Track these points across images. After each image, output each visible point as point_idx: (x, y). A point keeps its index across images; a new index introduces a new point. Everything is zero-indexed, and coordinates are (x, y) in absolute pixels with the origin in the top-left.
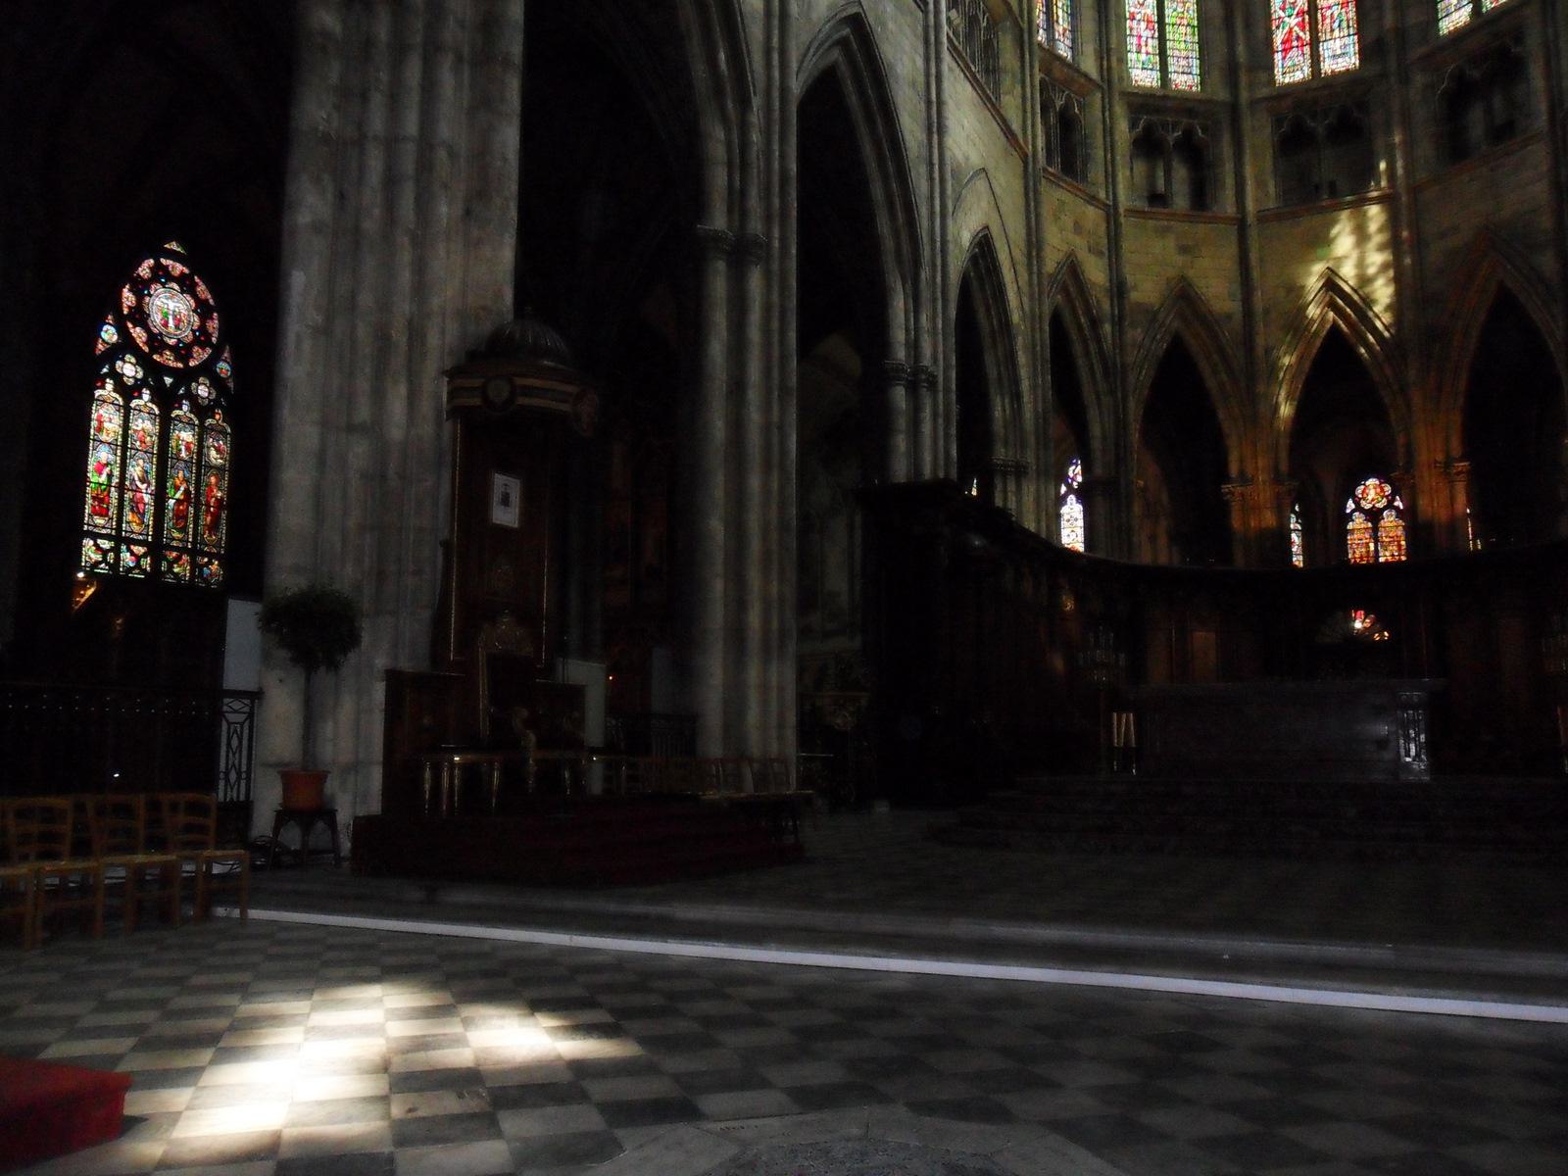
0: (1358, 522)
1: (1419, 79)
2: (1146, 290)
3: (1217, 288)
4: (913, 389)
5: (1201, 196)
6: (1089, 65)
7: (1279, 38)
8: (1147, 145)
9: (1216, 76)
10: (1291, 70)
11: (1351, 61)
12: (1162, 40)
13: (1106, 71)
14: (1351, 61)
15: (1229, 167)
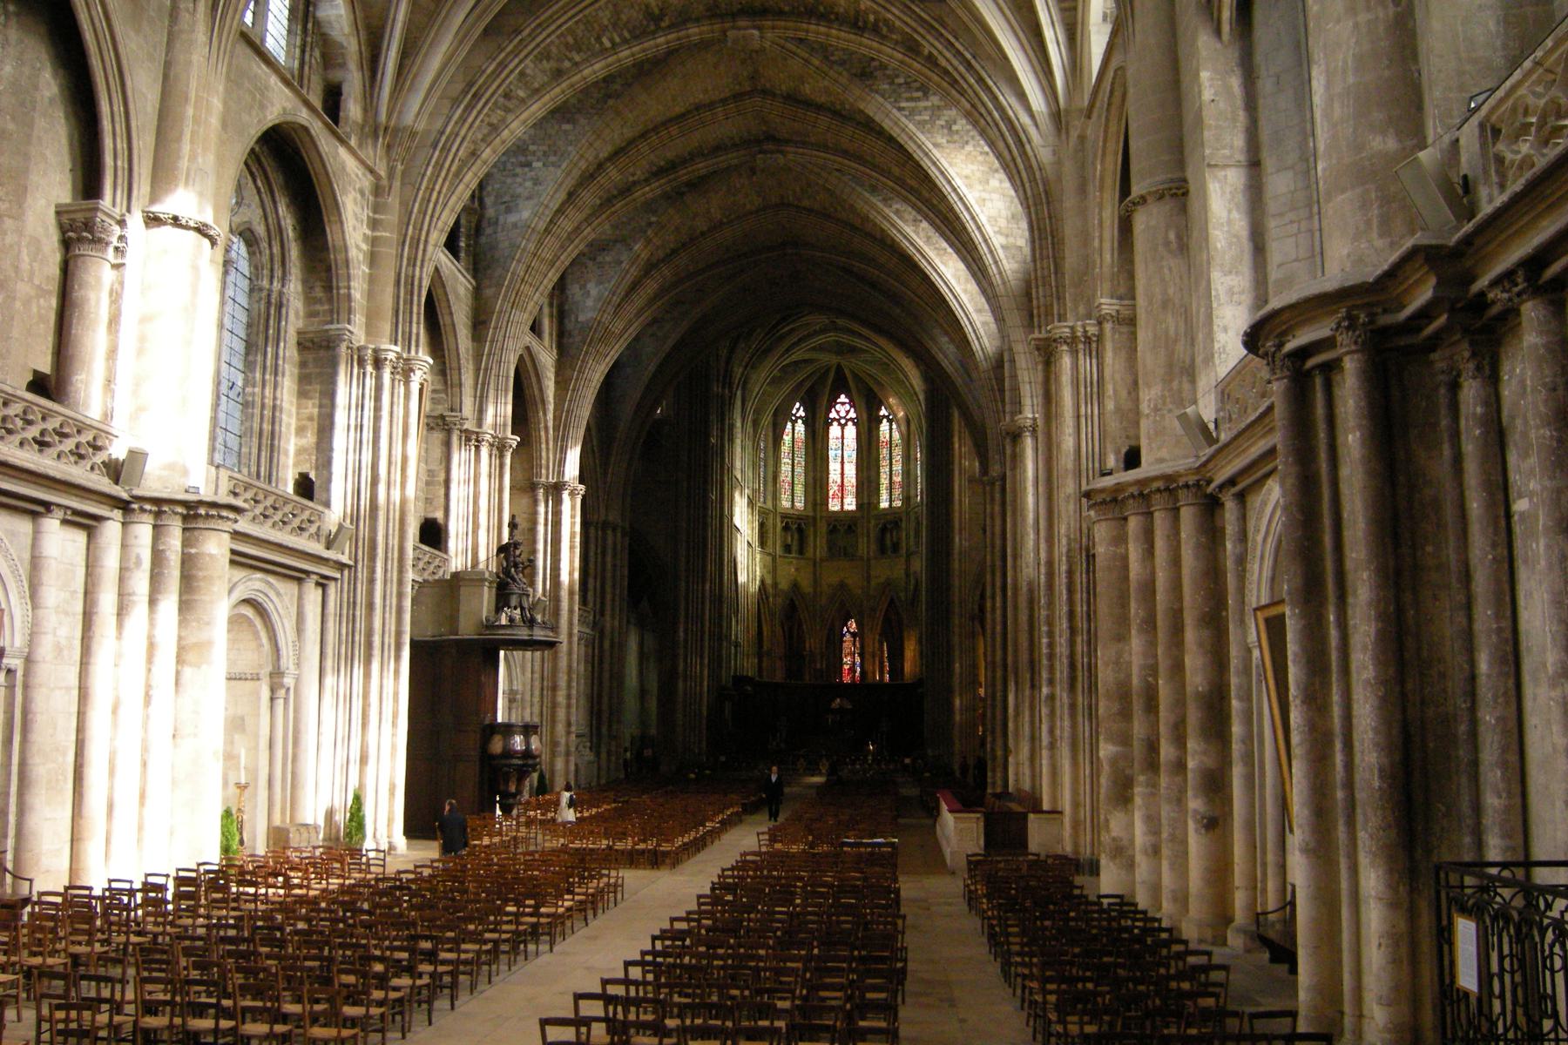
0: (848, 637)
1: (873, 522)
2: (784, 585)
3: (806, 585)
4: (736, 647)
5: (801, 551)
6: (769, 505)
7: (831, 493)
8: (786, 528)
9: (810, 506)
10: (834, 506)
11: (853, 507)
12: (793, 490)
13: (775, 506)
14: (853, 507)
15: (812, 538)
